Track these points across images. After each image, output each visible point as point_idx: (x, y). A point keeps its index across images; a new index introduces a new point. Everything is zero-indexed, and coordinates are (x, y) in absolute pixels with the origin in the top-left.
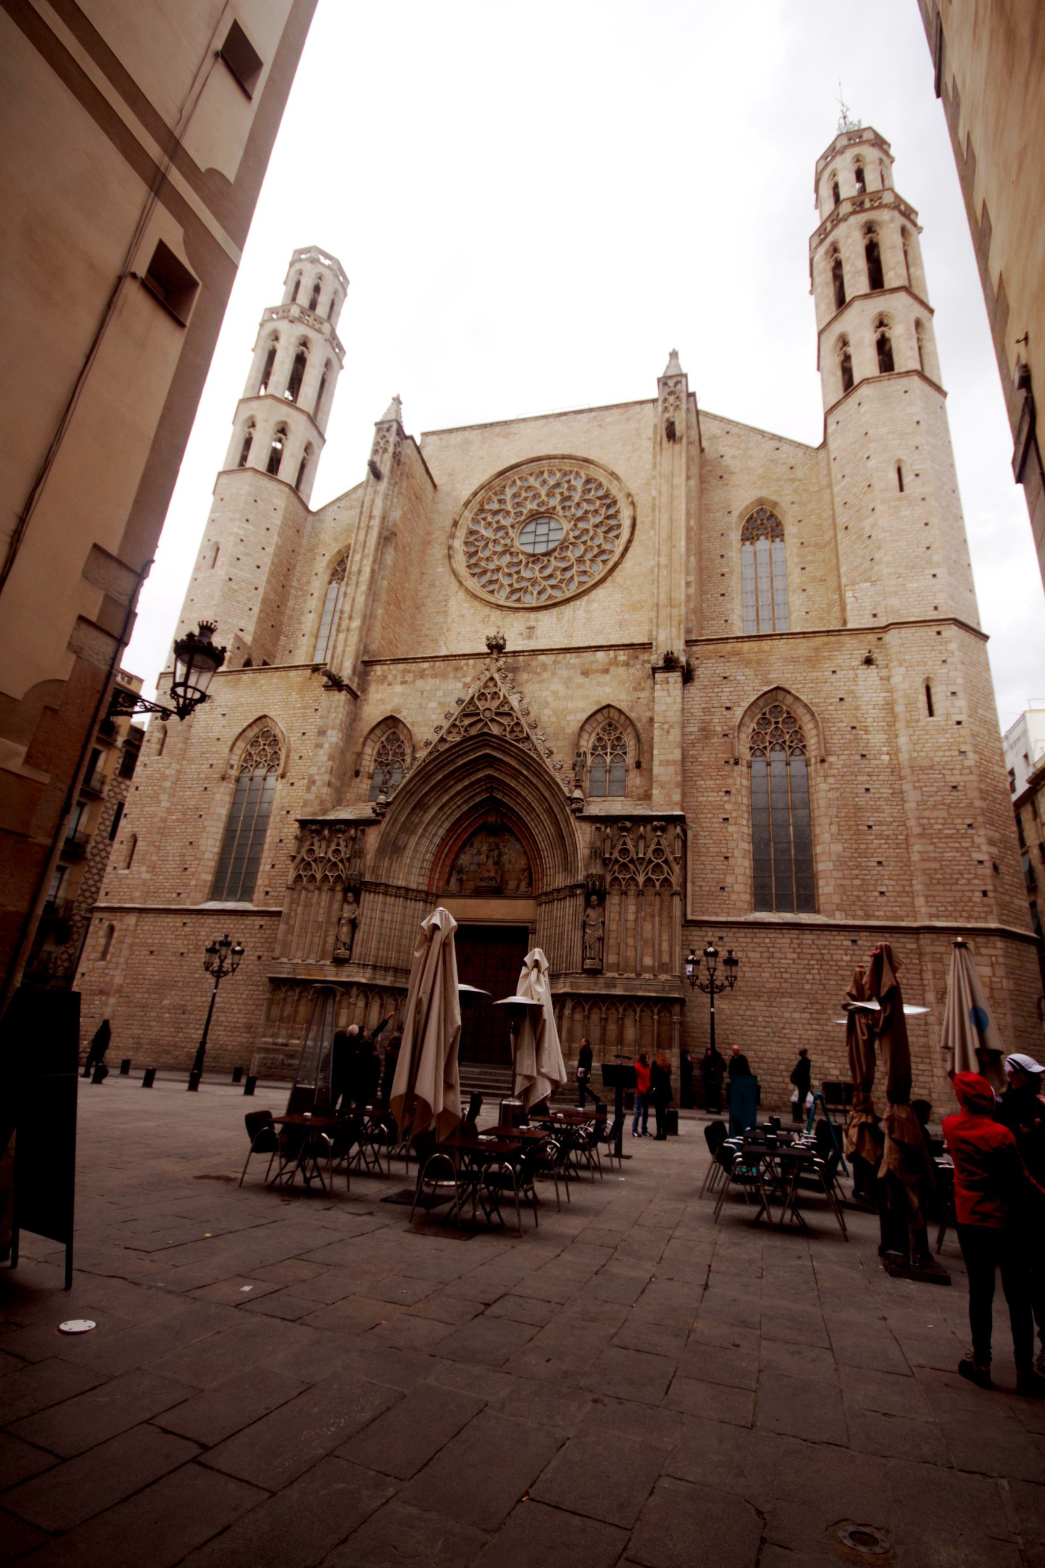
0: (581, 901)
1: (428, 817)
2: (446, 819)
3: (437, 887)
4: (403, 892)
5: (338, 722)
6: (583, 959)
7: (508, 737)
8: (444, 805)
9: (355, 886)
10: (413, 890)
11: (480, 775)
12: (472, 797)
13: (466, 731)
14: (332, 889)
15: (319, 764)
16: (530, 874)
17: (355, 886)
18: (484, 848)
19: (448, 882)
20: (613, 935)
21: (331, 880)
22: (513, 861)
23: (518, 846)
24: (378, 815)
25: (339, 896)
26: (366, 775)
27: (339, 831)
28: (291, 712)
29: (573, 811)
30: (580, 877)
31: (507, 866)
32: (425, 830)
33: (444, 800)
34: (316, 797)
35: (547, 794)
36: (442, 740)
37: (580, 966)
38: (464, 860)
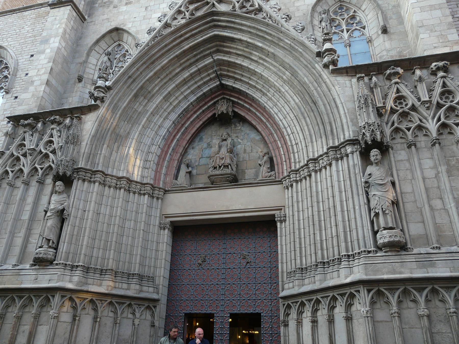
0: (356, 159)
1: (152, 106)
2: (172, 111)
3: (164, 183)
4: (124, 182)
5: (61, 31)
6: (375, 233)
7: (238, 12)
8: (169, 94)
9: (65, 174)
10: (137, 182)
11: (209, 60)
12: (199, 87)
13: (192, 14)
14: (41, 183)
15: (40, 67)
16: (271, 160)
17: (65, 174)
18: (214, 141)
19: (176, 177)
20: (408, 198)
21: (40, 172)
22: (248, 149)
23: (253, 135)
24: (95, 100)
25: (48, 189)
26: (90, 82)
27: (53, 122)
28: (22, 41)
29: (326, 66)
30: (349, 134)
31: (242, 155)
32: (149, 121)
33: (169, 89)
34: (33, 95)
35: (288, 60)
36: (167, 25)
37: (370, 242)
38: (192, 155)
